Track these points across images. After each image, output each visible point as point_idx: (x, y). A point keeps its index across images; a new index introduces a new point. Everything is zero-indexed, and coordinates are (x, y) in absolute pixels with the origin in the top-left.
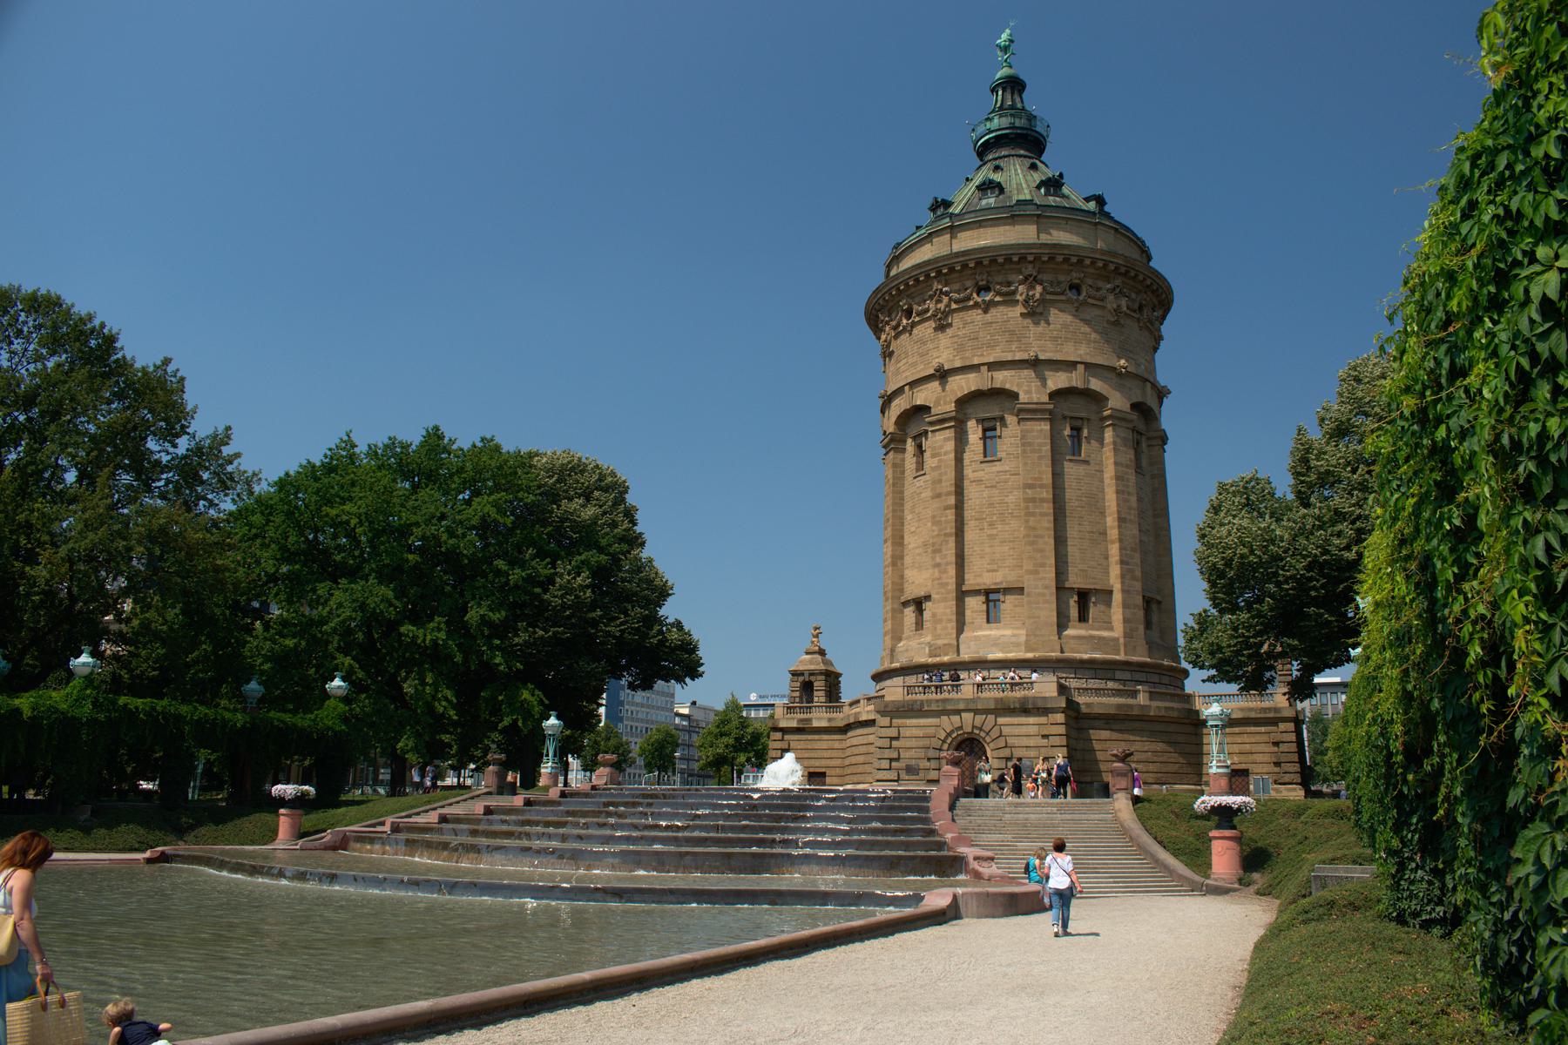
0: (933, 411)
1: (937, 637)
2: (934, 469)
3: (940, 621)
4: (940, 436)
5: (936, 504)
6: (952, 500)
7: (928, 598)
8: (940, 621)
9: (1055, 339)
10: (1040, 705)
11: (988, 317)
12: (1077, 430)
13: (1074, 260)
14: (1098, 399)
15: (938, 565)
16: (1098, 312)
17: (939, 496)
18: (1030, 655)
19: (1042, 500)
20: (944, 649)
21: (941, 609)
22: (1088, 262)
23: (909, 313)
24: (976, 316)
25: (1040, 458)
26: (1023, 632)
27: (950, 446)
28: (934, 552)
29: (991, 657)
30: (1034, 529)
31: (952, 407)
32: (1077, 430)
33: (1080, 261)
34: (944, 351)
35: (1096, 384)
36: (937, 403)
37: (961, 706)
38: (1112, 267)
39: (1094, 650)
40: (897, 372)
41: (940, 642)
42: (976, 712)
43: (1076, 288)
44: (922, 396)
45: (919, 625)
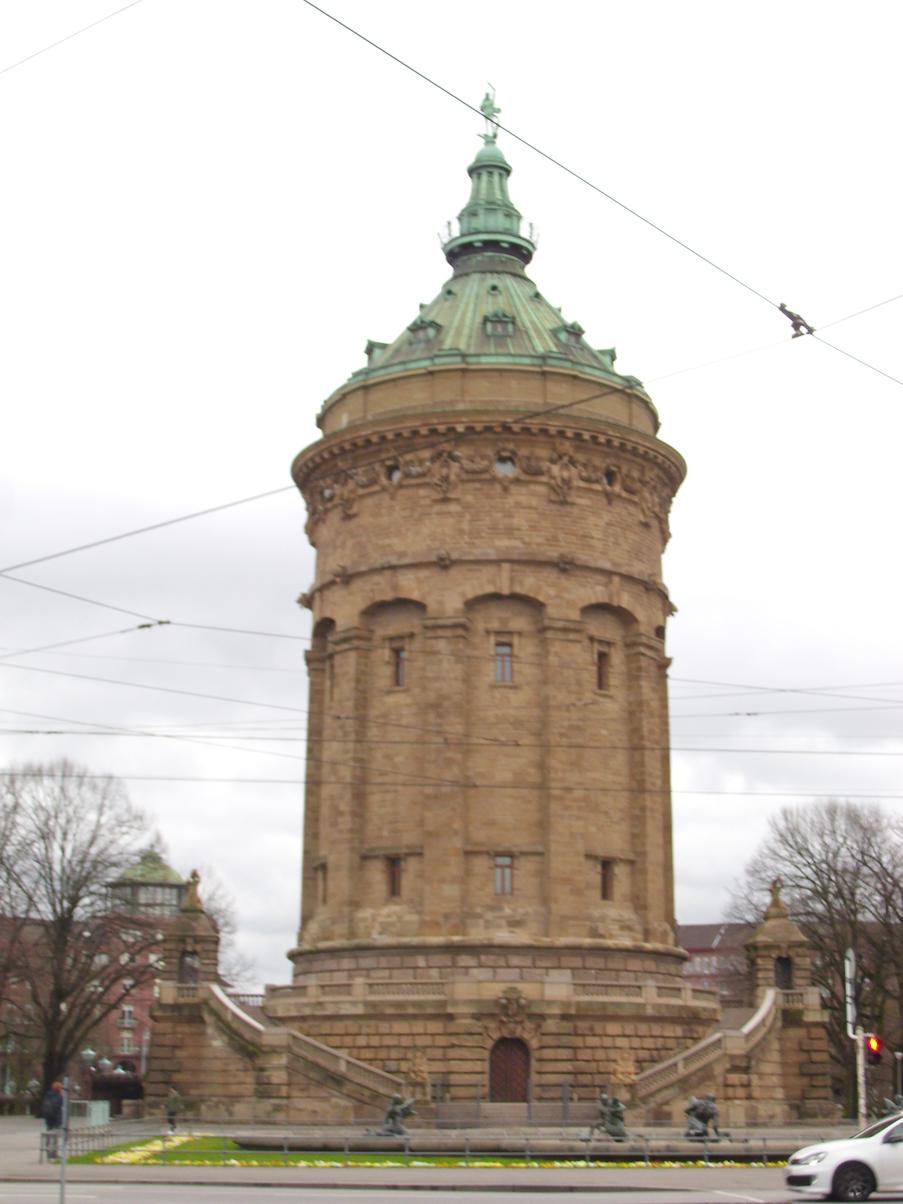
12: (603, 657)
14: (624, 617)
32: (603, 657)
35: (625, 600)
43: (610, 476)
44: (410, 585)
45: (394, 890)
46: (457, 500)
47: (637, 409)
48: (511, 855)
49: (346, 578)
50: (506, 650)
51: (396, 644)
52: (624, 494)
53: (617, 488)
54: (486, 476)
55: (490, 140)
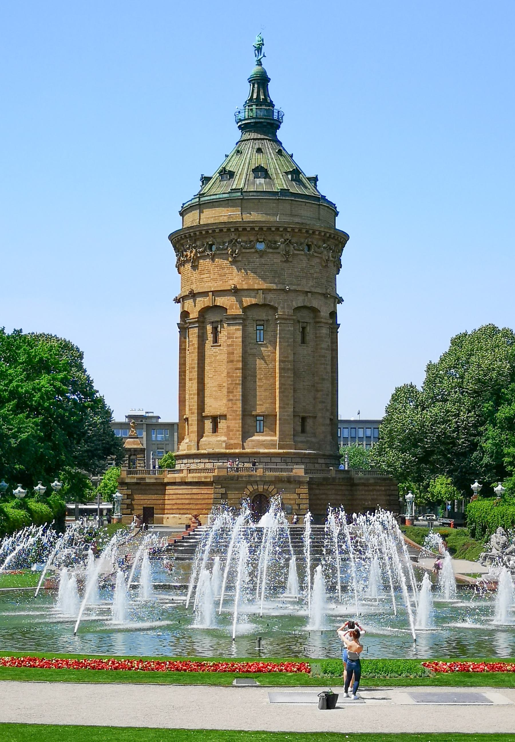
0: (229, 312)
1: (229, 439)
2: (229, 346)
3: (232, 431)
4: (233, 328)
5: (230, 365)
6: (240, 365)
7: (224, 417)
8: (232, 431)
9: (297, 277)
10: (297, 479)
11: (263, 260)
12: (304, 328)
13: (311, 232)
14: (314, 311)
15: (231, 400)
16: (318, 260)
17: (232, 361)
18: (281, 451)
19: (288, 369)
20: (235, 446)
21: (233, 424)
22: (317, 233)
23: (211, 246)
24: (257, 260)
25: (288, 346)
26: (277, 438)
27: (239, 334)
28: (228, 392)
29: (262, 451)
30: (285, 385)
31: (240, 312)
33: (314, 232)
34: (235, 278)
36: (231, 307)
37: (258, 479)
38: (328, 235)
39: (310, 449)
40: (201, 280)
41: (232, 442)
42: (265, 483)
45: (215, 429)
46: (240, 261)
47: (323, 212)
48: (263, 416)
49: (193, 295)
50: (262, 327)
51: (215, 325)
52: (315, 254)
53: (311, 252)
54: (253, 250)
55: (259, 63)
